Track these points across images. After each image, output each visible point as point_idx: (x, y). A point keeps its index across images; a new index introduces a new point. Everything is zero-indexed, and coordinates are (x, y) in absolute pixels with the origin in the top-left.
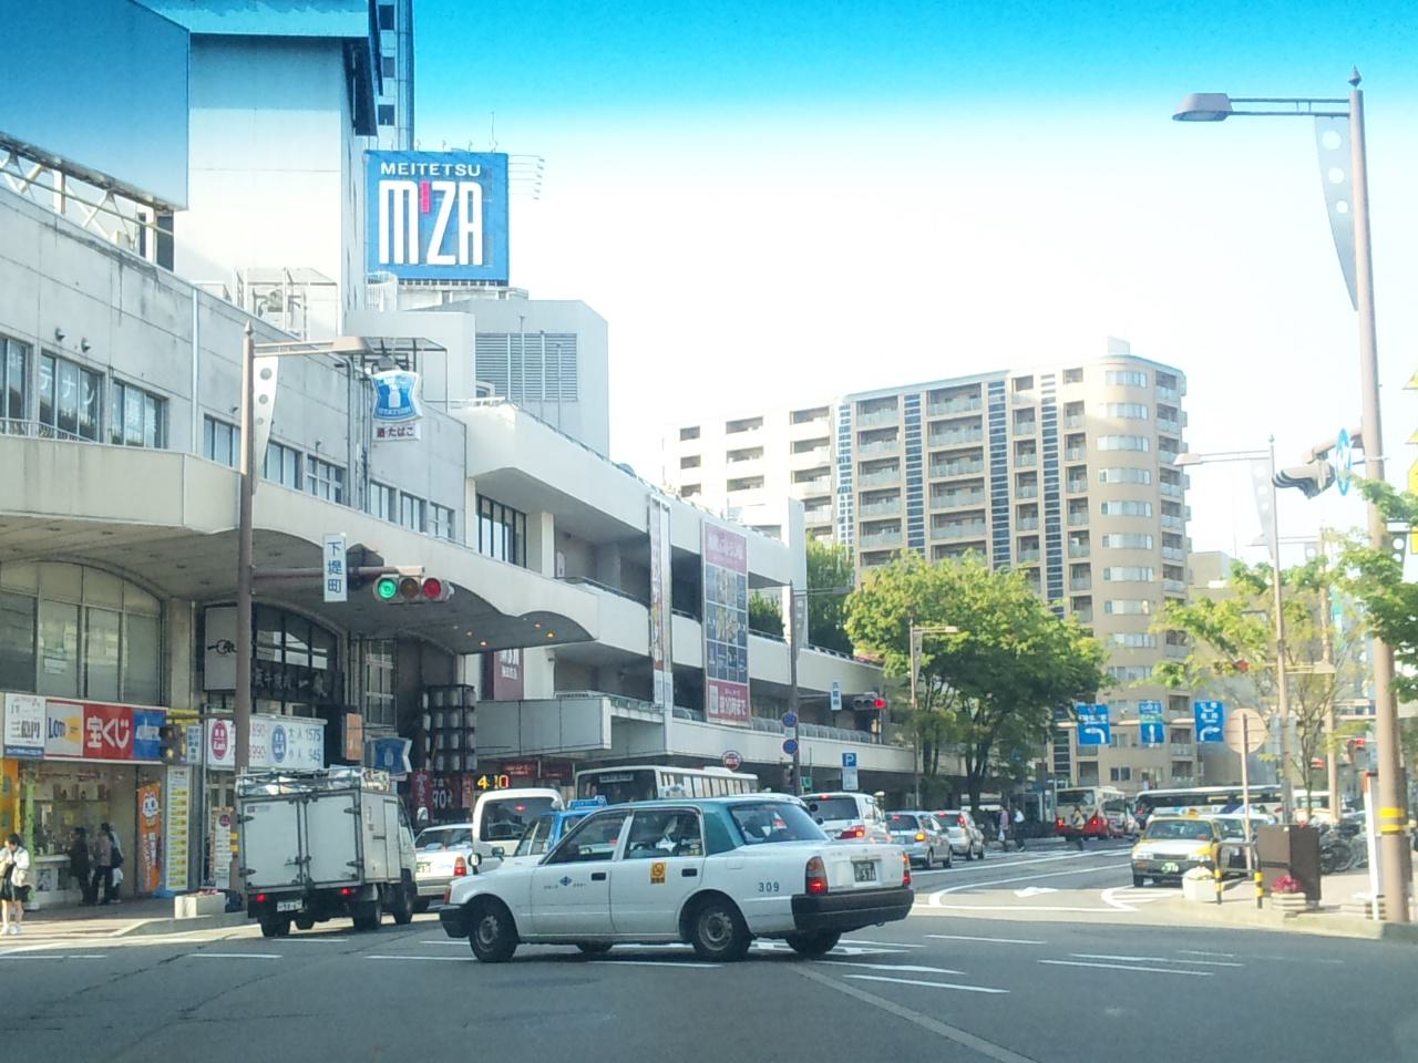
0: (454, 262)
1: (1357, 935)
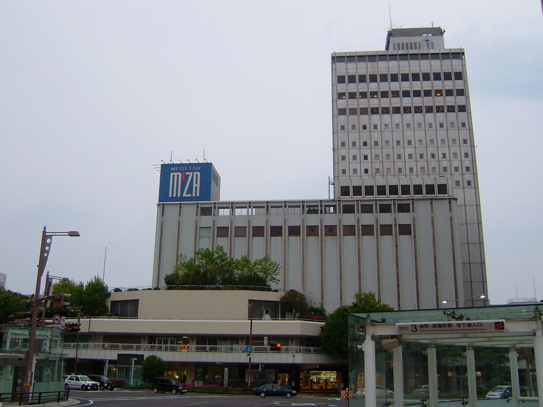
0: (191, 196)
1: (460, 113)
